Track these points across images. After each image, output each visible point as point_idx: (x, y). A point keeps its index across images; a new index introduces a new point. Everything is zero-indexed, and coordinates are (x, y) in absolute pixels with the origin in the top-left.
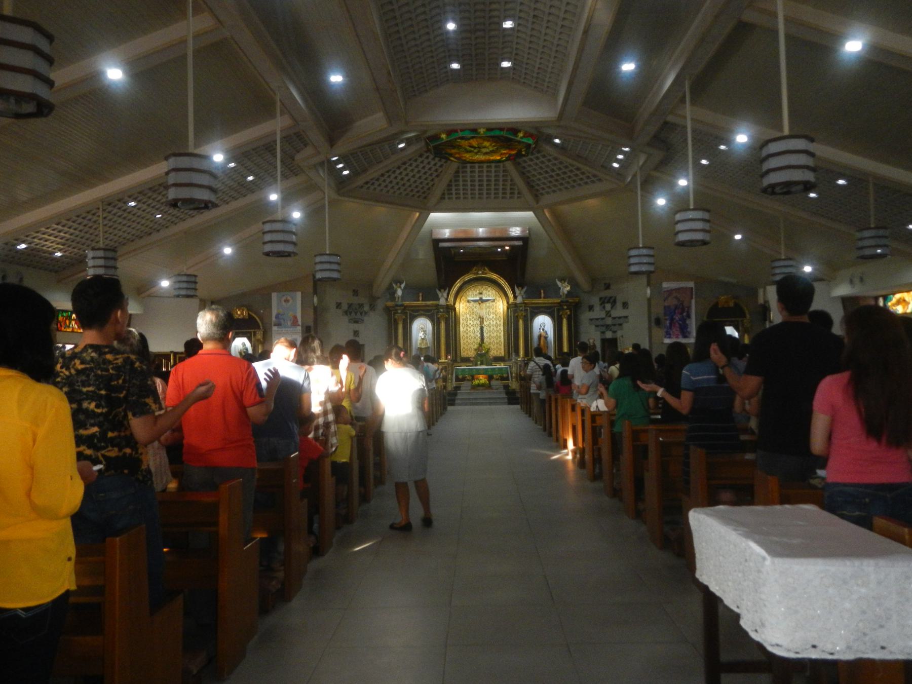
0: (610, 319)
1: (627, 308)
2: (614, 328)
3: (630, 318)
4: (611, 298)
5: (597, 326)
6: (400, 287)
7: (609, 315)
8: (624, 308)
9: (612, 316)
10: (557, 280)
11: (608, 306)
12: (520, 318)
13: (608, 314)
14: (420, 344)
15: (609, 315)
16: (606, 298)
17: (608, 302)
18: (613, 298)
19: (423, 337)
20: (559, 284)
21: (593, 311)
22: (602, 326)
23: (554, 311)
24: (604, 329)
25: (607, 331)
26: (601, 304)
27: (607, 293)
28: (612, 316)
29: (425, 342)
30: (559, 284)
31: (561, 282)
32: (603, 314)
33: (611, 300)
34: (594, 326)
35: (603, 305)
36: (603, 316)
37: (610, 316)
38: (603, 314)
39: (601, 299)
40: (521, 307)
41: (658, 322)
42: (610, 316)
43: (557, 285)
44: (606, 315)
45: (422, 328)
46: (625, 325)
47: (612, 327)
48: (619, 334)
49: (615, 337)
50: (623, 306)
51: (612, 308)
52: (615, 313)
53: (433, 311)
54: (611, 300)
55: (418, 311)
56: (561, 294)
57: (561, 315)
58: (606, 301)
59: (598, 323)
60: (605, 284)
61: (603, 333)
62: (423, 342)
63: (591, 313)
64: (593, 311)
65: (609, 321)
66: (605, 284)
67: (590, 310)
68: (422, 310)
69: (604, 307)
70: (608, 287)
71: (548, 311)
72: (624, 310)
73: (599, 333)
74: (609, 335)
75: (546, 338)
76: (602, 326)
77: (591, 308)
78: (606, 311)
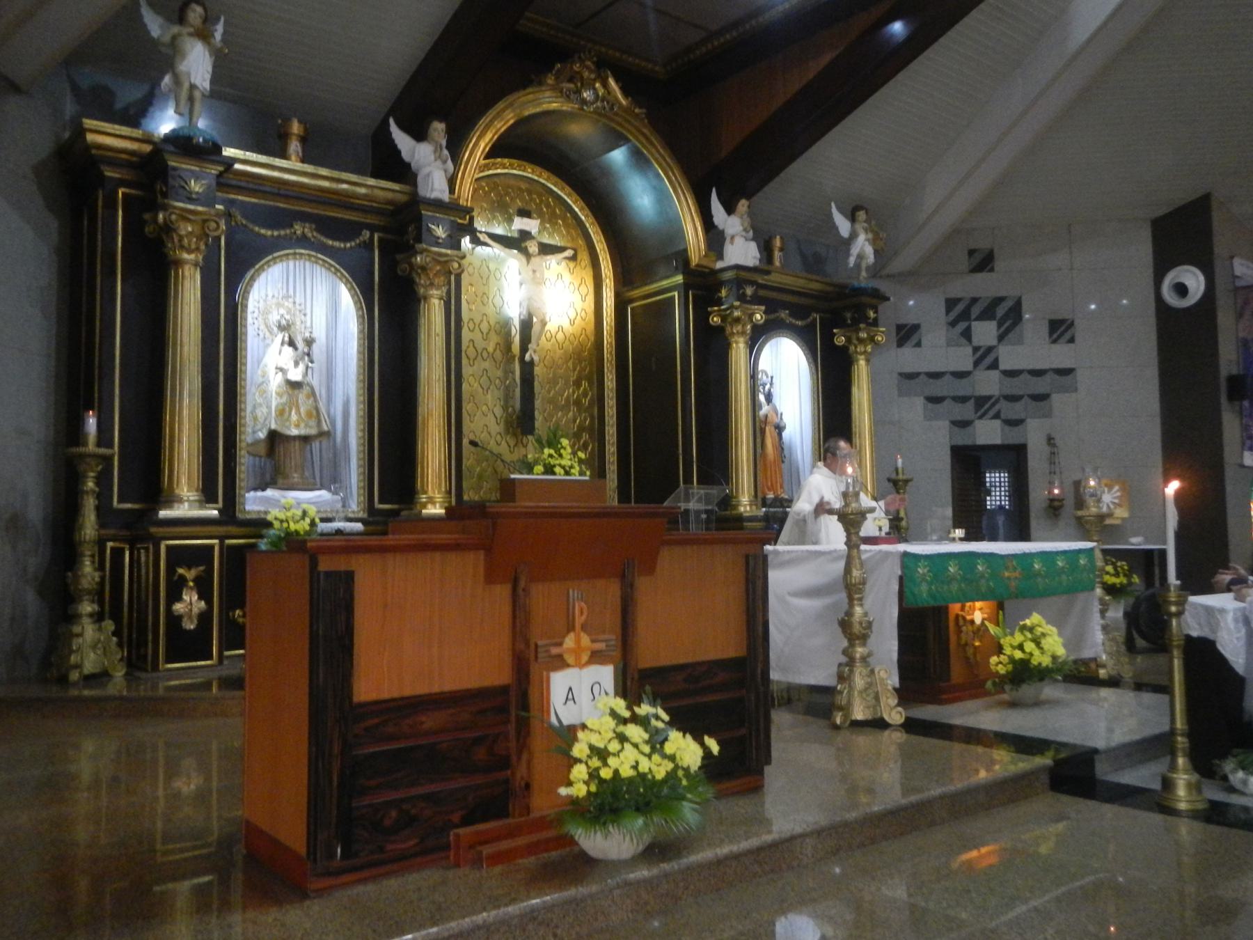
0: (995, 374)
1: (1072, 340)
2: (1010, 410)
3: (1082, 376)
4: (1000, 300)
5: (934, 400)
6: (203, 35)
7: (988, 360)
8: (1054, 341)
9: (1002, 366)
10: (833, 205)
11: (985, 332)
12: (743, 333)
13: (985, 358)
14: (281, 412)
15: (988, 360)
16: (974, 300)
17: (987, 314)
18: (1008, 304)
19: (296, 375)
20: (843, 226)
21: (918, 344)
22: (963, 400)
23: (813, 324)
24: (967, 411)
25: (981, 417)
26: (953, 324)
27: (984, 286)
28: (1002, 366)
29: (302, 396)
30: (843, 226)
31: (853, 219)
32: (962, 358)
33: (1001, 311)
34: (919, 402)
35: (962, 326)
36: (967, 365)
37: (994, 365)
38: (962, 358)
39: (951, 304)
40: (752, 283)
41: (1237, 388)
42: (994, 365)
43: (834, 228)
44: (976, 364)
45: (282, 328)
46: (1056, 399)
47: (1003, 406)
48: (1034, 435)
49: (1013, 437)
50: (1051, 334)
51: (1001, 338)
52: (1010, 357)
53: (366, 234)
54: (1001, 311)
55: (280, 219)
56: (852, 261)
57: (844, 349)
58: (976, 311)
59: (938, 388)
60: (971, 253)
61: (963, 424)
62: (293, 404)
63: (907, 352)
64: (918, 344)
65: (988, 383)
66: (971, 253)
67: (901, 343)
68: (304, 217)
69: (967, 334)
70: (984, 262)
71: (799, 323)
72: (1056, 348)
73: (943, 426)
74: (988, 432)
75: (780, 429)
76: (963, 400)
77: (906, 334)
78: (976, 349)
